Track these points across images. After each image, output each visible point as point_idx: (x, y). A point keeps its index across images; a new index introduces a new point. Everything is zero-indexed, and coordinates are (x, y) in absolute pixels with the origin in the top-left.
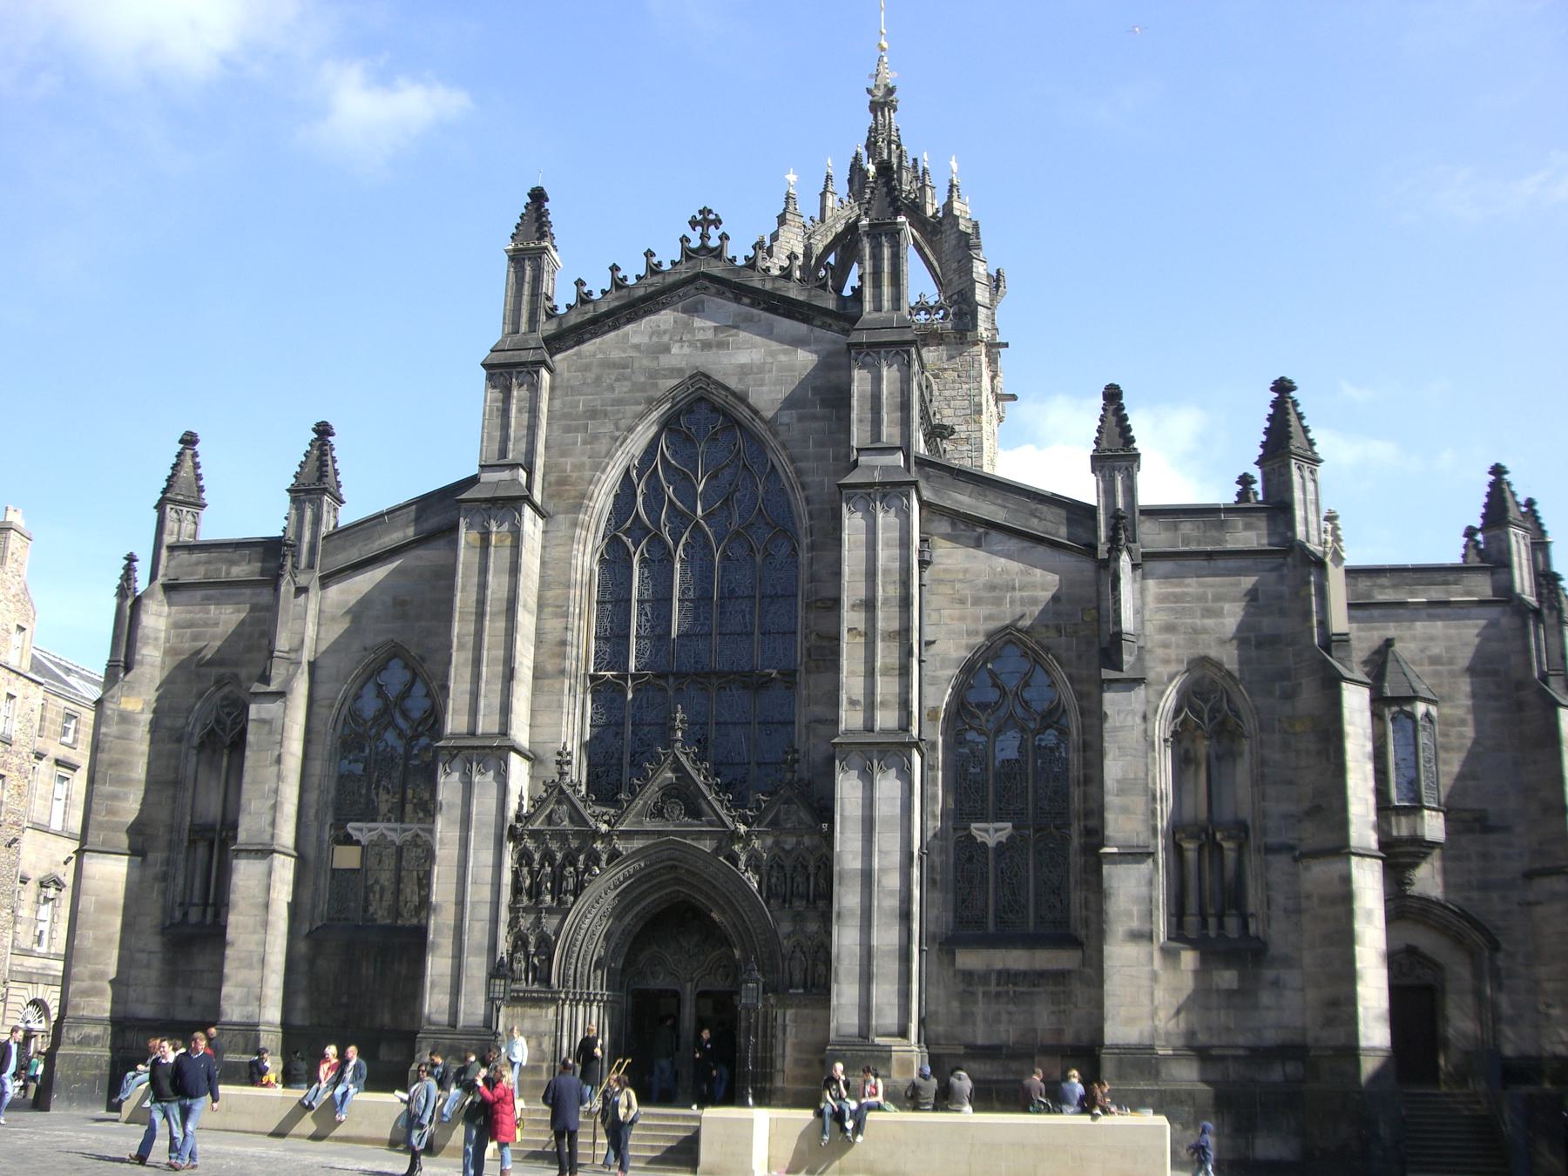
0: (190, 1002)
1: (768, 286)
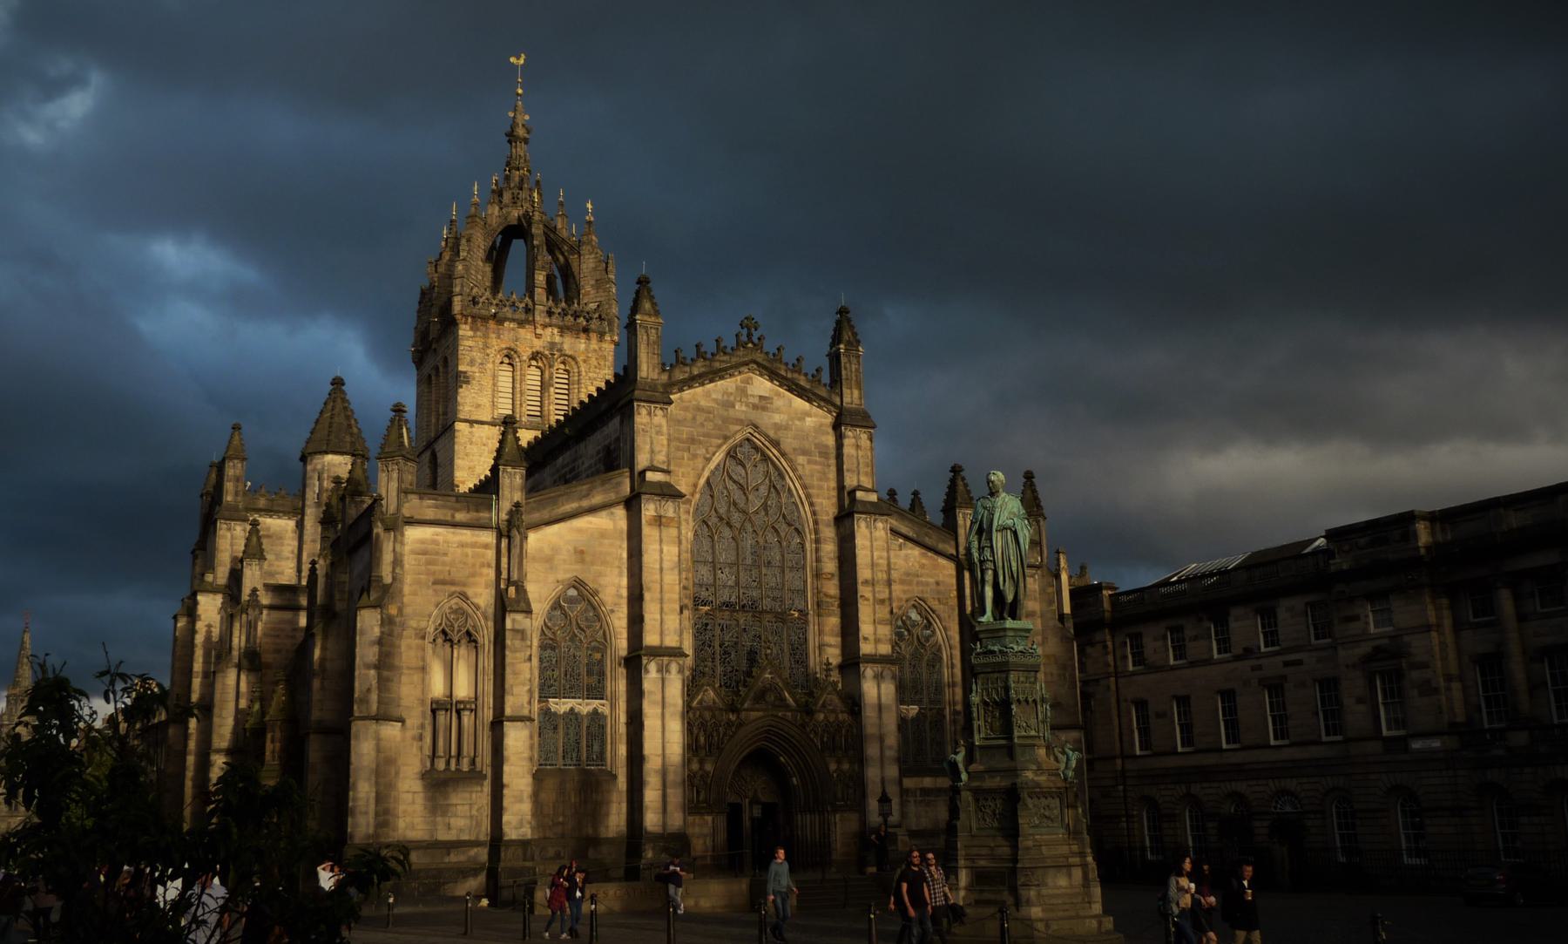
0: (449, 827)
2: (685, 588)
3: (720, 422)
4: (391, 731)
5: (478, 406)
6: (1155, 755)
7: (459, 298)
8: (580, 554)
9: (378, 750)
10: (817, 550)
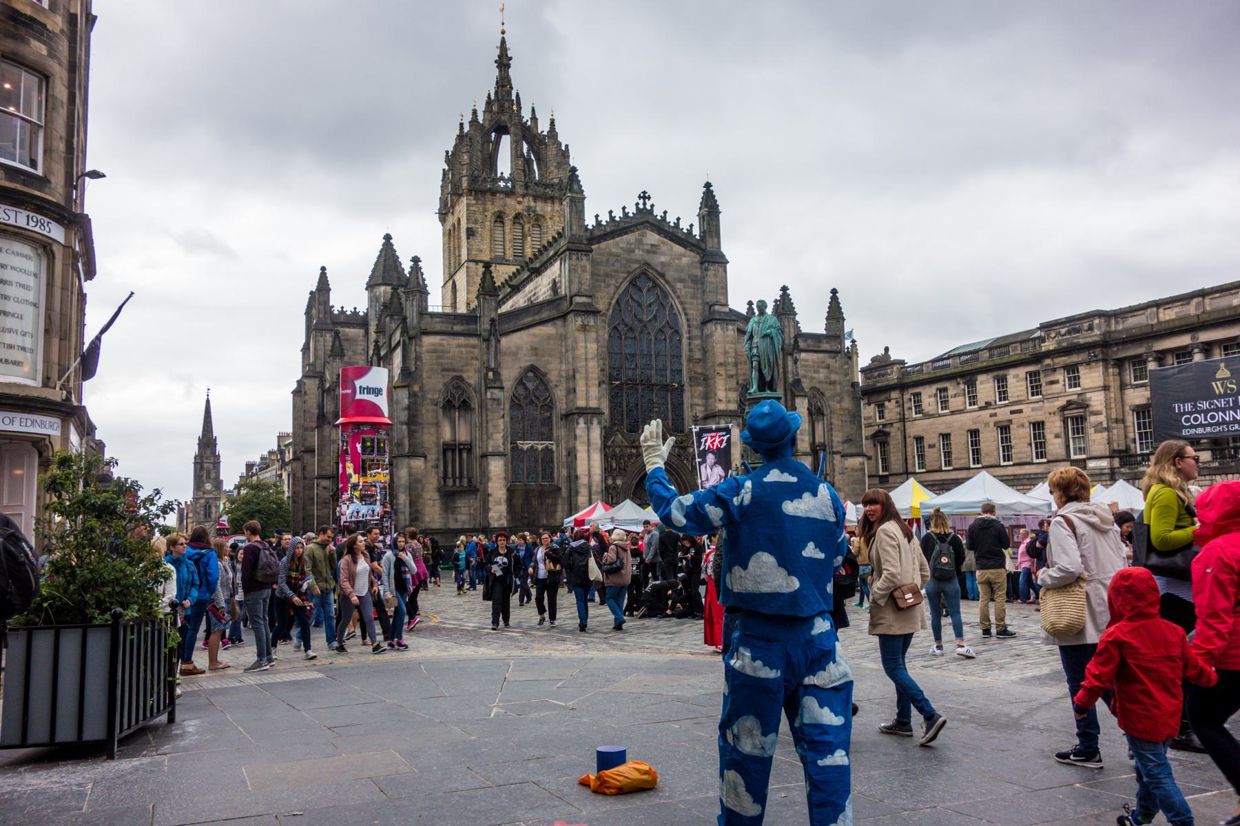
0: (456, 521)
1: (671, 230)
2: (602, 370)
3: (625, 262)
4: (418, 463)
5: (481, 251)
6: (928, 472)
7: (466, 178)
8: (535, 350)
9: (410, 474)
10: (690, 344)
